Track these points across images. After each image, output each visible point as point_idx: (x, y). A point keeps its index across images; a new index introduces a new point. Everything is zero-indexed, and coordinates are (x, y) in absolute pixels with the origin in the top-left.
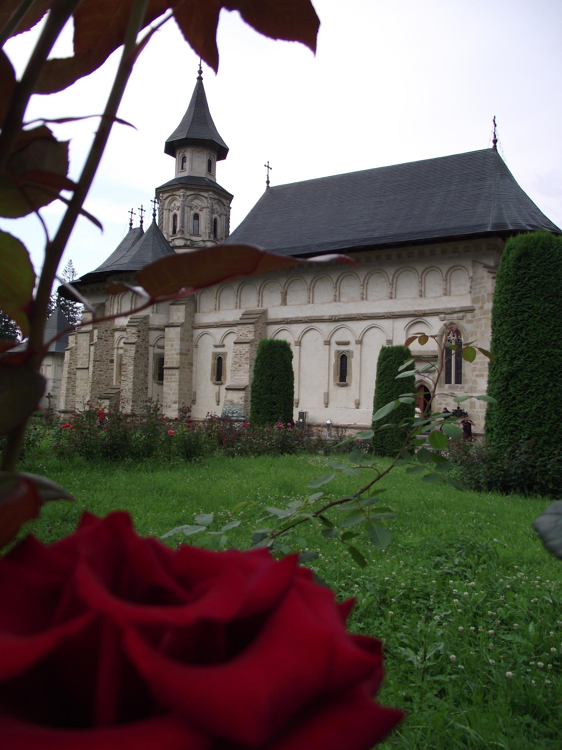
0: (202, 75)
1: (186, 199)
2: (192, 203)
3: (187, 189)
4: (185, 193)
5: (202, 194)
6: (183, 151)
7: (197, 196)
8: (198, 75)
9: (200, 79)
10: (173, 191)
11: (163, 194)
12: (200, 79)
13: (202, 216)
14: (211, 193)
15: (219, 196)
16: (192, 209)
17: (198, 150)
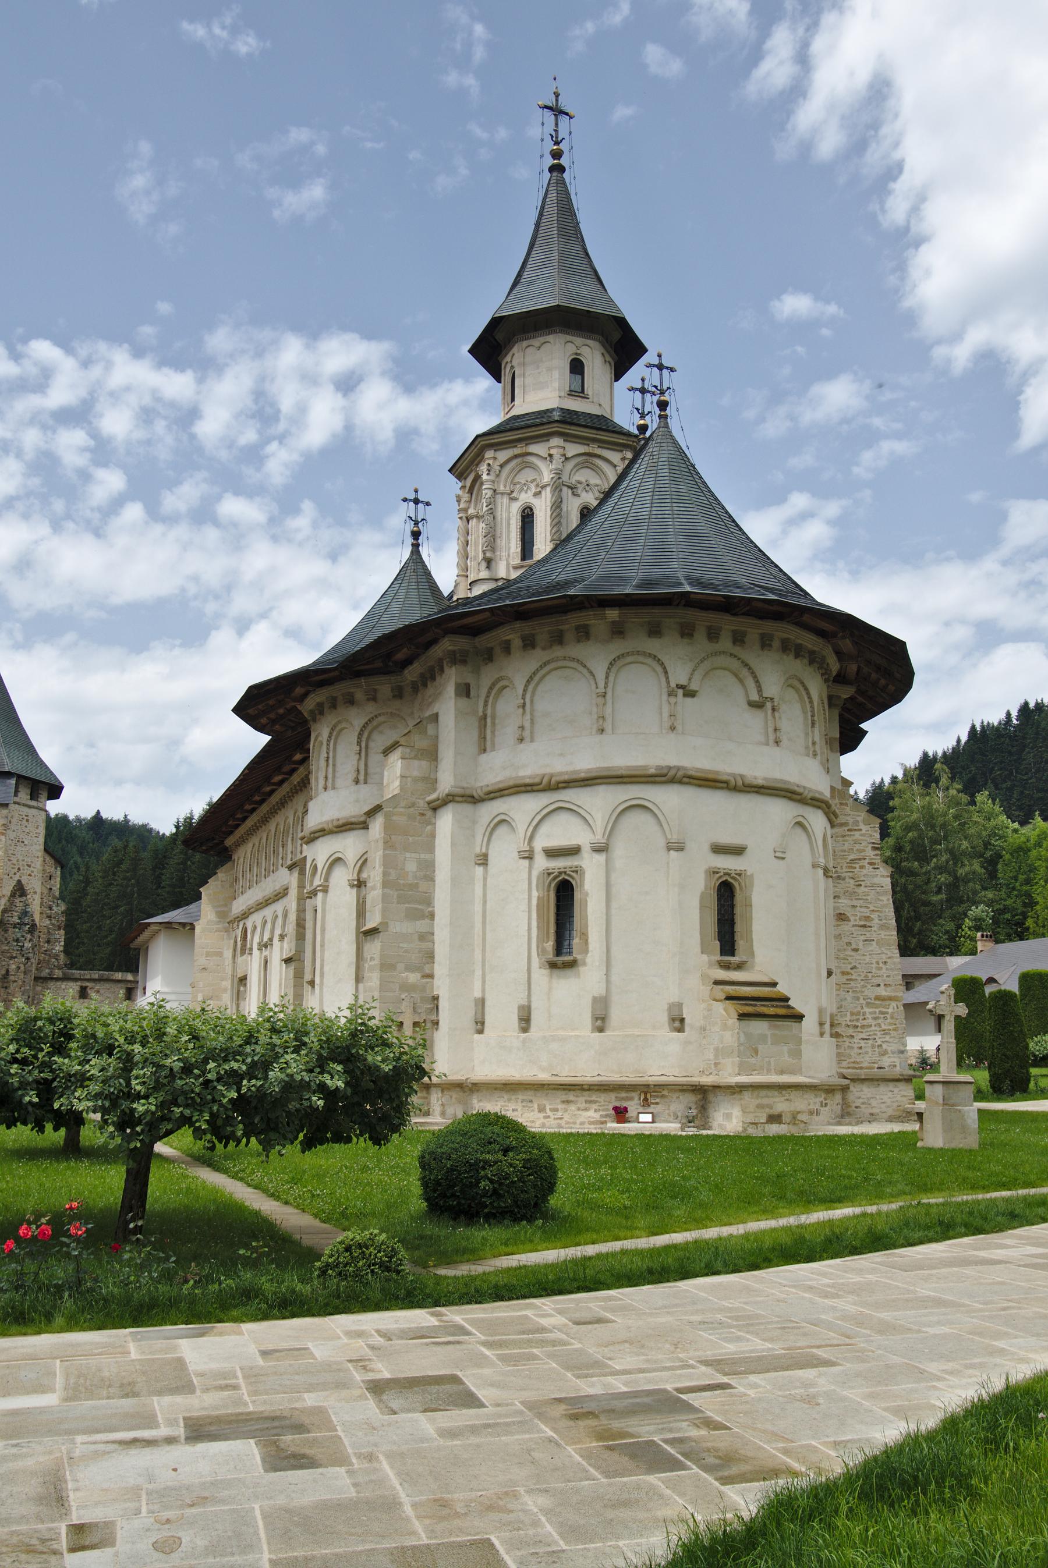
0: (564, 161)
1: (498, 476)
2: (516, 480)
3: (497, 446)
4: (495, 458)
5: (533, 448)
6: (508, 358)
7: (523, 460)
8: (550, 161)
9: (557, 169)
10: (477, 465)
11: (465, 479)
12: (557, 169)
13: (538, 508)
14: (556, 441)
15: (588, 445)
16: (516, 499)
17: (536, 342)
